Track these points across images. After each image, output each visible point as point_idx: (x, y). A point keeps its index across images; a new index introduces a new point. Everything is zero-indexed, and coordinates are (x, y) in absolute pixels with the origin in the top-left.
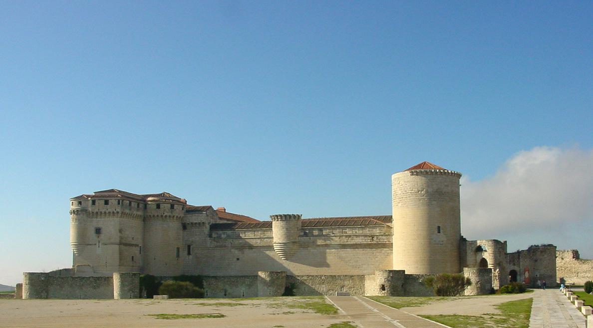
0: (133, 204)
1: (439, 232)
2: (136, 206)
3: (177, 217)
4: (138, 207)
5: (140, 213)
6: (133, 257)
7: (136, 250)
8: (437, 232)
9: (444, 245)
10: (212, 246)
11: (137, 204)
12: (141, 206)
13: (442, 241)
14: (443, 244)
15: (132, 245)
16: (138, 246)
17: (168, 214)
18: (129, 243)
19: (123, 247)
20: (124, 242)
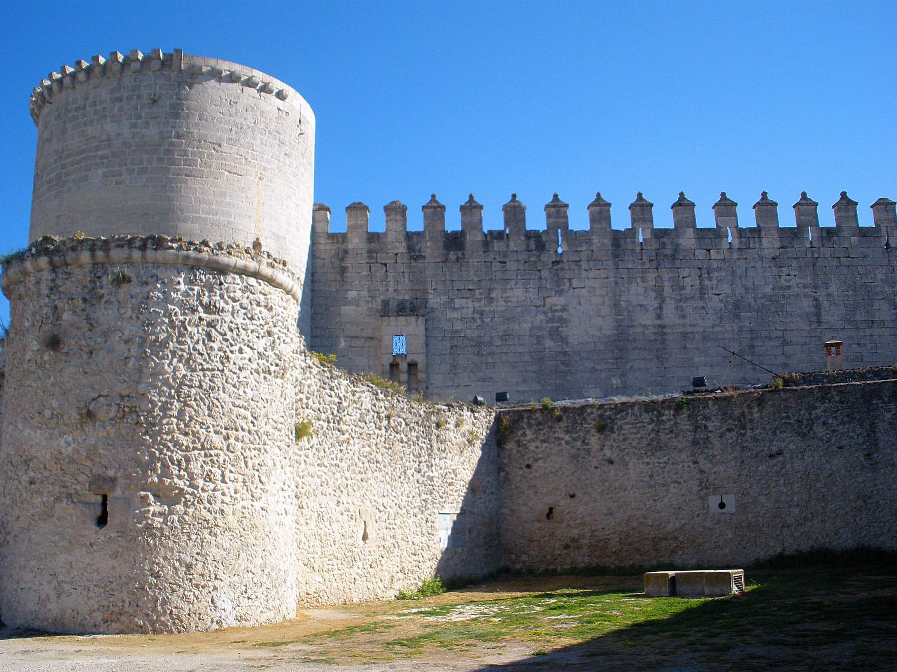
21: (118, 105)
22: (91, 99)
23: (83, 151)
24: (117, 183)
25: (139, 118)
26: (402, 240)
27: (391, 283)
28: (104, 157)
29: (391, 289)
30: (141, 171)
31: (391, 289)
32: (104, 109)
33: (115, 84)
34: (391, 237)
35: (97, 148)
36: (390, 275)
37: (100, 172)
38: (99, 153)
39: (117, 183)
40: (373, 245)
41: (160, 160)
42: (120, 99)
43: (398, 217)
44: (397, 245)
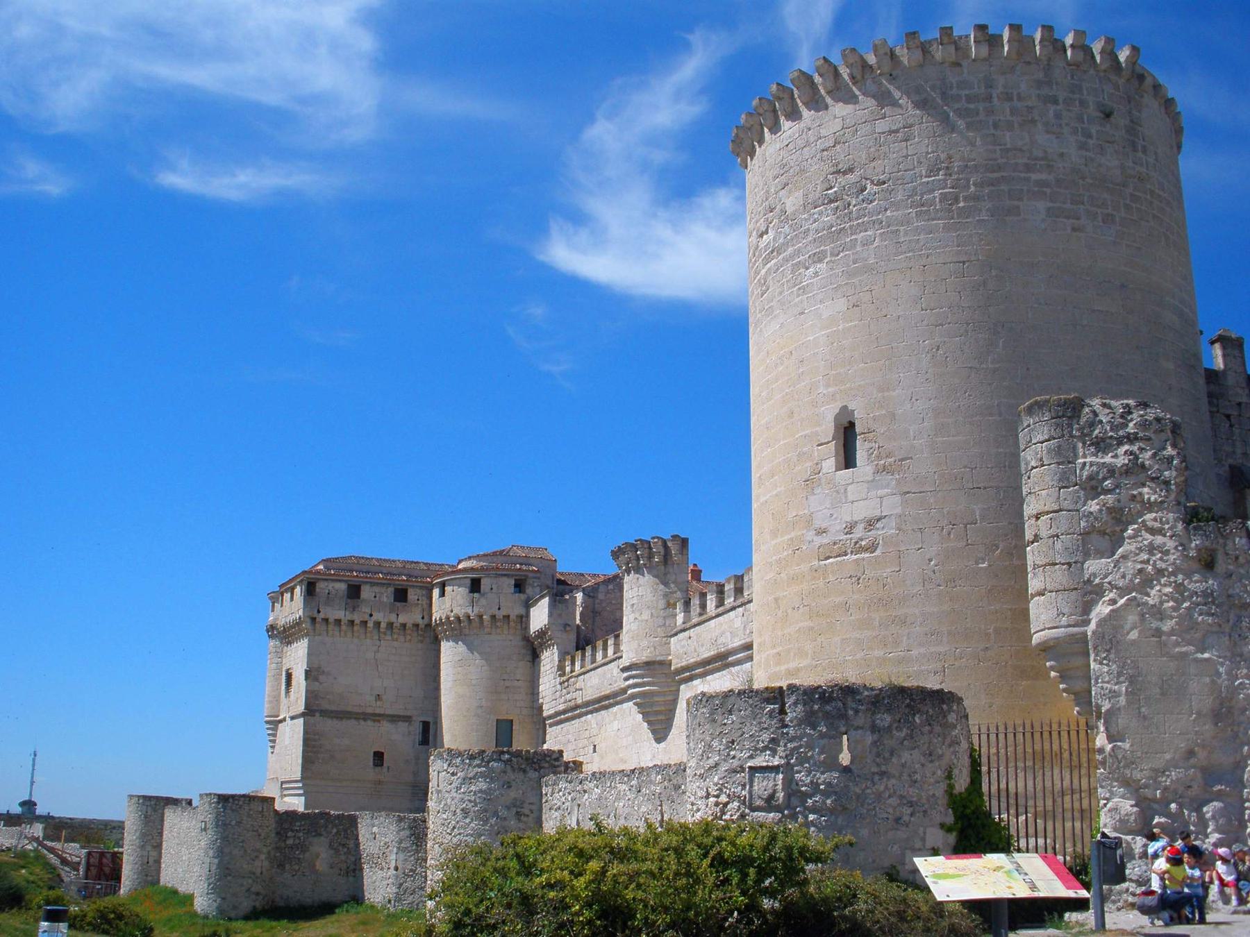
0: (366, 592)
1: (848, 460)
2: (387, 595)
3: (493, 617)
4: (401, 595)
5: (410, 616)
6: (379, 757)
7: (398, 739)
8: (829, 464)
9: (878, 552)
10: (561, 707)
11: (391, 590)
12: (412, 595)
13: (871, 523)
14: (872, 548)
15: (377, 717)
16: (407, 719)
17: (459, 611)
18: (357, 710)
19: (329, 725)
20: (325, 705)
21: (1052, 109)
22: (1000, 89)
23: (1000, 168)
24: (1074, 229)
25: (1090, 136)
26: (1244, 385)
27: (1238, 444)
28: (1044, 184)
29: (1239, 451)
30: (1108, 219)
31: (1239, 451)
32: (1030, 109)
33: (1041, 75)
34: (1231, 380)
35: (1028, 168)
36: (1236, 431)
37: (1041, 205)
38: (1034, 177)
39: (1074, 229)
40: (1212, 387)
41: (1127, 207)
42: (1056, 102)
43: (1236, 352)
44: (1240, 391)
